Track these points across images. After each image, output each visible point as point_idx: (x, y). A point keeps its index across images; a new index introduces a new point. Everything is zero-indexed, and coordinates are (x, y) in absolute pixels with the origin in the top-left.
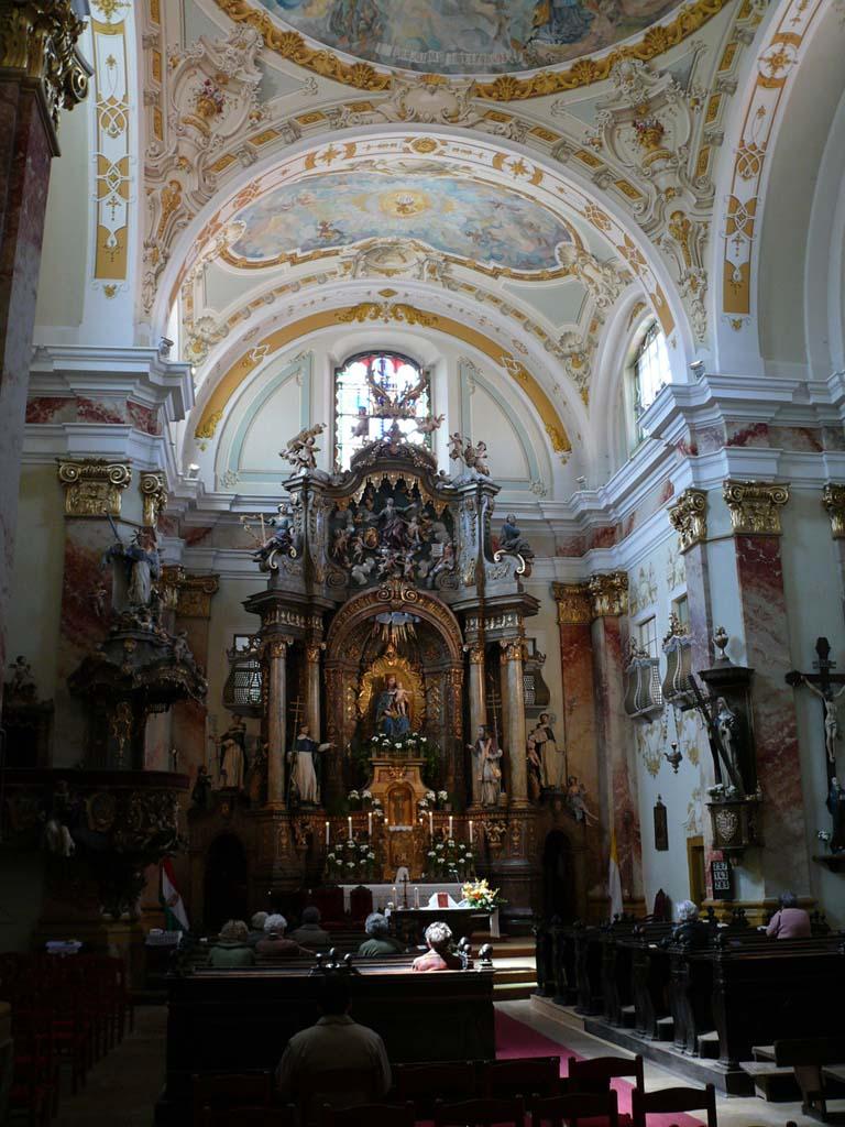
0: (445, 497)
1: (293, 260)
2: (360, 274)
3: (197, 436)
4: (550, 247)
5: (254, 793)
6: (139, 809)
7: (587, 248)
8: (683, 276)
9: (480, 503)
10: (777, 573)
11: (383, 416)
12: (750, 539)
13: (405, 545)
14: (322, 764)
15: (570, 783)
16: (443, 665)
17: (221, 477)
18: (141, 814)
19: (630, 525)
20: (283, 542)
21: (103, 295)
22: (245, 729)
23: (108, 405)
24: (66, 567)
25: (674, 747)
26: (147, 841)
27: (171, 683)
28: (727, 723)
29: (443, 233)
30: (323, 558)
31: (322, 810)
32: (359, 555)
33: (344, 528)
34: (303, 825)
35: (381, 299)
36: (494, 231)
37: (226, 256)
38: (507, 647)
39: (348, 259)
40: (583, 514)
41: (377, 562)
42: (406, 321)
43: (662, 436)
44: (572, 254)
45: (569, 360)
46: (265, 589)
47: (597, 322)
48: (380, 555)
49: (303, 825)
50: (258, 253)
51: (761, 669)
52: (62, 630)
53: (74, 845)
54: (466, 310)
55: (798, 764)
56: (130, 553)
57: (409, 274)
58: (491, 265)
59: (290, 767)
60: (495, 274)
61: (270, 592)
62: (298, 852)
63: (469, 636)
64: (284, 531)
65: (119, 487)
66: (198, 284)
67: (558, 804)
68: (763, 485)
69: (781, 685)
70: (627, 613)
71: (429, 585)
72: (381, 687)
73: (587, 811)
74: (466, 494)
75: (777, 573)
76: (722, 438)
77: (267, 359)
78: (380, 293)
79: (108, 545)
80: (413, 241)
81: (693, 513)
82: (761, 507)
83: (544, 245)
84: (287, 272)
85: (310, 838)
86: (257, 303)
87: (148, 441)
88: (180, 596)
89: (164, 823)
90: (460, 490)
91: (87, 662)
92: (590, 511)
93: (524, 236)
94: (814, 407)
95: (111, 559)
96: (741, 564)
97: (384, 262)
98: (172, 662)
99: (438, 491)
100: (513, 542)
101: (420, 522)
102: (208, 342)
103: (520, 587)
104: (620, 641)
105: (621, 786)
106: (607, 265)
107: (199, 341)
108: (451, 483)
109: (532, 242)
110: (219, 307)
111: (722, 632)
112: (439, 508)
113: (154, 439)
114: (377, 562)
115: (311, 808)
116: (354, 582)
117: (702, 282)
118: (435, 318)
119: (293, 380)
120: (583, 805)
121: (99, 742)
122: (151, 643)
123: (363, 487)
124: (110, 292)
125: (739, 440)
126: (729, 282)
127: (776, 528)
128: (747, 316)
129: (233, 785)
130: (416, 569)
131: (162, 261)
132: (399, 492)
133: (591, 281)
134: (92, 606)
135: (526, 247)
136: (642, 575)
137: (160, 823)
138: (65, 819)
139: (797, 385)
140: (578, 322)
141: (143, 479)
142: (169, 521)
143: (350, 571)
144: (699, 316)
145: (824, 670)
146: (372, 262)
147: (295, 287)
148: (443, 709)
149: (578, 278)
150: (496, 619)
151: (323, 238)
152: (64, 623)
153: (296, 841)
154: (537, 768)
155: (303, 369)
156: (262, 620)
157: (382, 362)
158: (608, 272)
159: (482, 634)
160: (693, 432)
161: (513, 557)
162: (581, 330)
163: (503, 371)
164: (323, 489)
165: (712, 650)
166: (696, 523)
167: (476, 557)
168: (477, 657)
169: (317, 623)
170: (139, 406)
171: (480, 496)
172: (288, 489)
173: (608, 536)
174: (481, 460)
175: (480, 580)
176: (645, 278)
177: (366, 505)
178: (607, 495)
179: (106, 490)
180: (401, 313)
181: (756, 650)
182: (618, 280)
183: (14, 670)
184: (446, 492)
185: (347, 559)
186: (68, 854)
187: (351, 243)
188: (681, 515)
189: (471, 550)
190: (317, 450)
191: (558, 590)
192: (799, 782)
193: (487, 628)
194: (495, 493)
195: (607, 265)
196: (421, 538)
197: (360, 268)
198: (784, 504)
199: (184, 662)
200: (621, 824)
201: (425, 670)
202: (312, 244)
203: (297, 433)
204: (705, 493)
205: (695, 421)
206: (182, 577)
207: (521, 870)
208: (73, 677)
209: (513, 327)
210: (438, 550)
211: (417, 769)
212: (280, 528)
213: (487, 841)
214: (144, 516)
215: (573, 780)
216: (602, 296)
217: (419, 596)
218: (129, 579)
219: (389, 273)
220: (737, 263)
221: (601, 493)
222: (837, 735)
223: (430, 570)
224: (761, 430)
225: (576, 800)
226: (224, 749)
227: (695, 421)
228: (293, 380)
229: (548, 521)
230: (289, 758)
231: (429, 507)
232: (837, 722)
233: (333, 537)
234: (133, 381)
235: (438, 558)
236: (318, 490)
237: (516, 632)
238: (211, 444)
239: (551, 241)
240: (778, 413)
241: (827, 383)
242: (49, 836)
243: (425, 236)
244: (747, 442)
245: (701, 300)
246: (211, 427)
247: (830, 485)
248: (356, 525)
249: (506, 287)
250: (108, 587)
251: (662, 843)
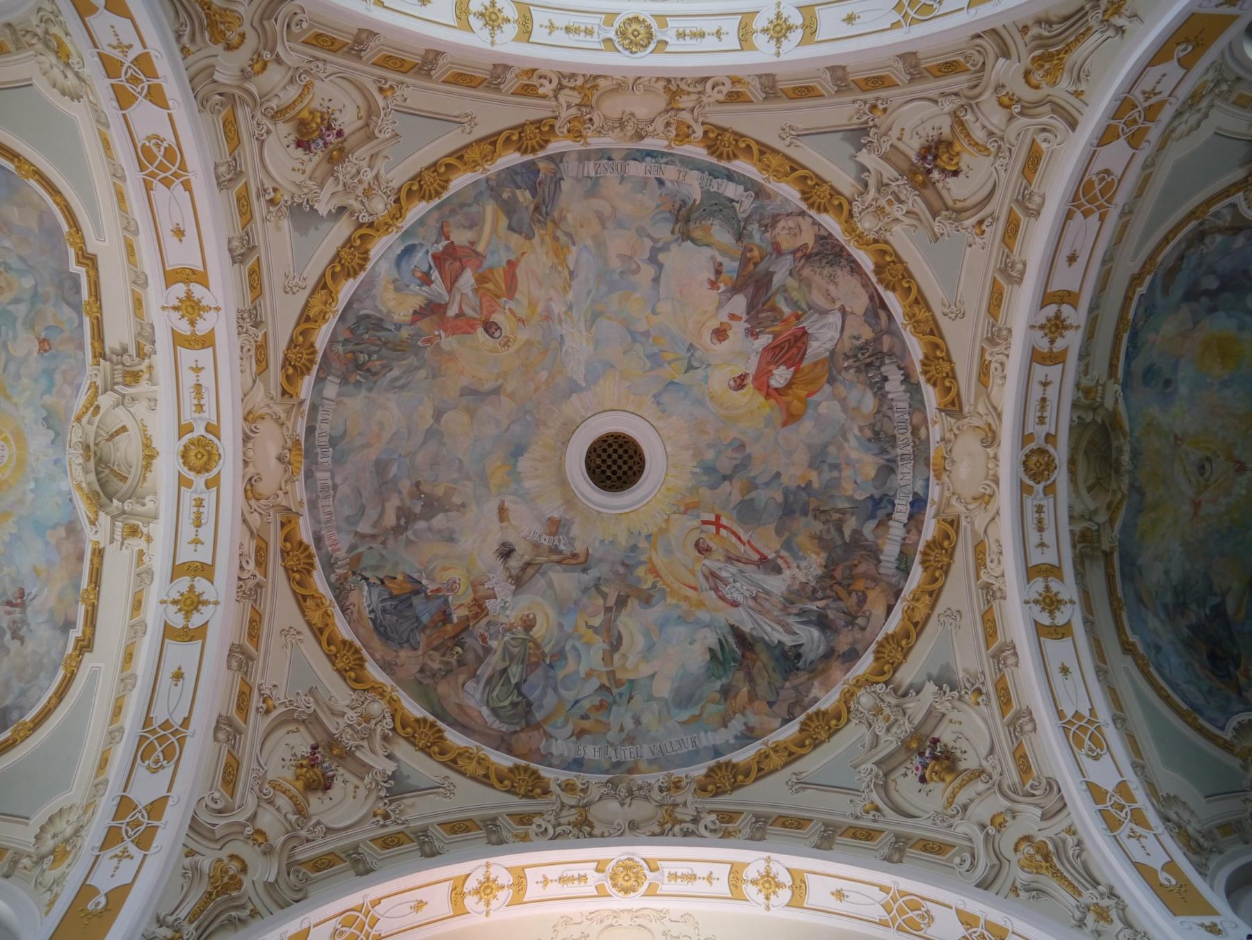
2: (150, 506)
39: (118, 531)
60: (88, 260)
197: (139, 508)
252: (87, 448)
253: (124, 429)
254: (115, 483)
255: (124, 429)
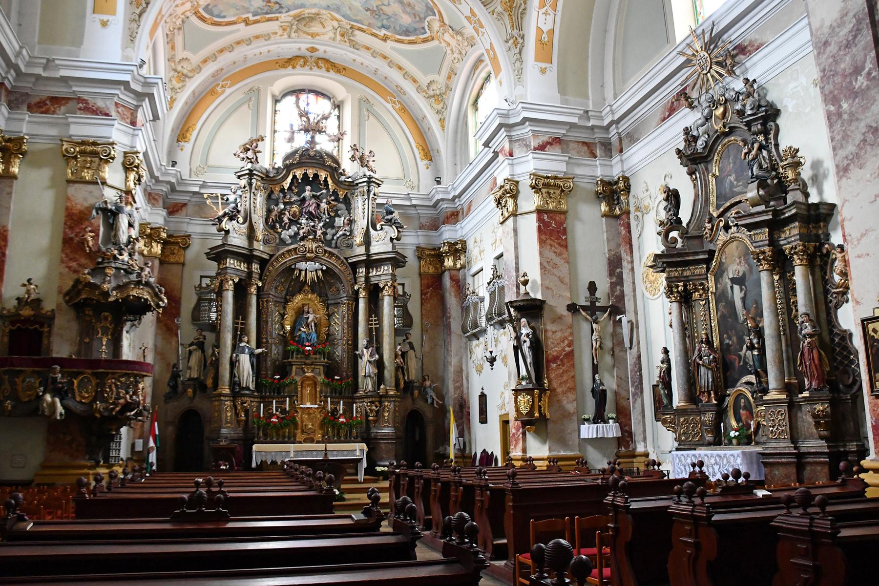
0: (346, 187)
1: (247, 22)
3: (178, 141)
4: (422, 20)
5: (209, 382)
6: (113, 385)
7: (447, 21)
8: (508, 37)
9: (369, 191)
10: (564, 238)
11: (307, 131)
12: (546, 213)
13: (318, 218)
14: (258, 362)
15: (424, 380)
16: (341, 298)
17: (194, 169)
18: (114, 389)
19: (469, 209)
20: (233, 212)
21: (99, 25)
22: (205, 339)
23: (100, 103)
24: (66, 216)
25: (491, 352)
26: (118, 409)
27: (139, 298)
28: (528, 335)
29: (350, 8)
30: (262, 225)
31: (256, 394)
32: (286, 223)
33: (277, 205)
34: (242, 403)
35: (308, 54)
36: (383, 8)
37: (199, 15)
38: (384, 287)
40: (438, 201)
41: (299, 229)
42: (324, 69)
43: (490, 145)
44: (436, 25)
45: (433, 100)
46: (220, 243)
47: (452, 74)
48: (301, 224)
49: (242, 403)
50: (222, 15)
51: (550, 302)
52: (62, 261)
53: (63, 411)
54: (364, 64)
55: (573, 365)
56: (114, 208)
57: (326, 37)
58: (382, 32)
59: (233, 364)
60: (385, 39)
61: (224, 245)
62: (239, 422)
63: (358, 280)
64: (234, 205)
65: (107, 162)
66: (179, 35)
67: (416, 392)
68: (556, 178)
69: (565, 312)
70: (465, 268)
71: (333, 245)
72: (300, 312)
73: (434, 397)
74: (359, 185)
75: (564, 238)
76: (530, 146)
77: (228, 91)
78: (307, 49)
79: (99, 204)
80: (330, 14)
81: (508, 195)
82: (554, 193)
83: (418, 19)
84: (242, 31)
85: (247, 412)
86: (221, 51)
87: (131, 131)
88: (163, 250)
89: (131, 397)
90: (356, 182)
91: (77, 282)
92: (443, 200)
93: (405, 12)
94: (593, 128)
95: (100, 212)
96: (540, 230)
97: (310, 27)
98: (138, 283)
99: (341, 182)
100: (389, 217)
101: (328, 203)
102: (186, 76)
103: (394, 247)
104: (460, 287)
105: (458, 382)
106: (459, 33)
107: (180, 74)
108: (349, 177)
109: (410, 16)
110: (194, 53)
111: (525, 275)
112: (341, 194)
113: (134, 130)
114: (299, 229)
115: (247, 392)
116: (283, 242)
117: (521, 41)
118: (344, 69)
119: (246, 106)
120: (432, 394)
121: (87, 340)
122: (125, 270)
123: (291, 177)
124: (104, 24)
125: (542, 148)
126: (539, 41)
127: (564, 207)
128: (551, 65)
129: (196, 377)
130: (325, 234)
131: (144, 5)
132: (315, 182)
133: (449, 44)
134: (84, 244)
135: (406, 20)
136: (475, 242)
137: (128, 396)
138: (58, 392)
139: (582, 112)
140: (439, 73)
141: (125, 157)
142: (156, 197)
143: (280, 234)
144: (518, 64)
145: (593, 303)
146: (301, 26)
147: (249, 41)
148: (340, 328)
149: (440, 43)
150: (377, 269)
151: (268, 8)
152: (63, 256)
153: (237, 414)
154: (402, 368)
155: (253, 99)
156: (219, 265)
157: (307, 97)
158: (460, 38)
159: (367, 278)
160: (510, 141)
161: (390, 228)
162: (441, 79)
163: (389, 106)
164: (262, 178)
165: (518, 287)
166: (510, 202)
167: (365, 228)
168: (362, 294)
169: (255, 267)
170: (124, 106)
171: (369, 187)
172: (239, 177)
173: (454, 217)
174: (371, 163)
175: (367, 242)
176: (483, 39)
177: (292, 190)
178: (454, 189)
179: (97, 163)
180: (321, 64)
181: (547, 288)
182: (466, 44)
183: (24, 289)
184: (347, 184)
185: (278, 225)
186: (58, 418)
187: (287, 12)
188: (501, 197)
189: (361, 223)
190: (260, 152)
191: (420, 251)
192: (573, 377)
193: (371, 275)
194: (379, 185)
195: (459, 33)
196: (329, 214)
197: (293, 30)
198: (570, 191)
199: (147, 284)
200: (458, 406)
201: (329, 302)
202: (260, 11)
203: (245, 139)
204: (518, 182)
205: (513, 134)
206: (164, 235)
207: (389, 435)
208: (67, 294)
209: (396, 76)
210: (339, 221)
211: (322, 368)
212: (231, 203)
213: (367, 416)
214: (126, 184)
215: (427, 377)
216: (456, 55)
217: (326, 251)
218: (112, 227)
219: (313, 35)
220: (545, 29)
221: (450, 187)
222: (600, 346)
223: (334, 235)
224: (557, 141)
225: (429, 390)
226: (190, 352)
227: (513, 134)
228: (246, 106)
229: (415, 206)
230: (234, 358)
231: (335, 193)
232: (600, 338)
233: (269, 211)
234: (118, 87)
235: (340, 227)
236: (260, 179)
237: (390, 277)
238: (188, 146)
239: (422, 16)
240: (568, 131)
241: (601, 112)
242: (45, 405)
243: (338, 10)
244: (547, 149)
245: (520, 53)
246: (188, 135)
247: (601, 180)
248: (285, 204)
249: (393, 48)
250: (96, 231)
251: (484, 420)
252: (318, 15)
253: (324, 27)
254: (304, 22)
255: (324, 27)
